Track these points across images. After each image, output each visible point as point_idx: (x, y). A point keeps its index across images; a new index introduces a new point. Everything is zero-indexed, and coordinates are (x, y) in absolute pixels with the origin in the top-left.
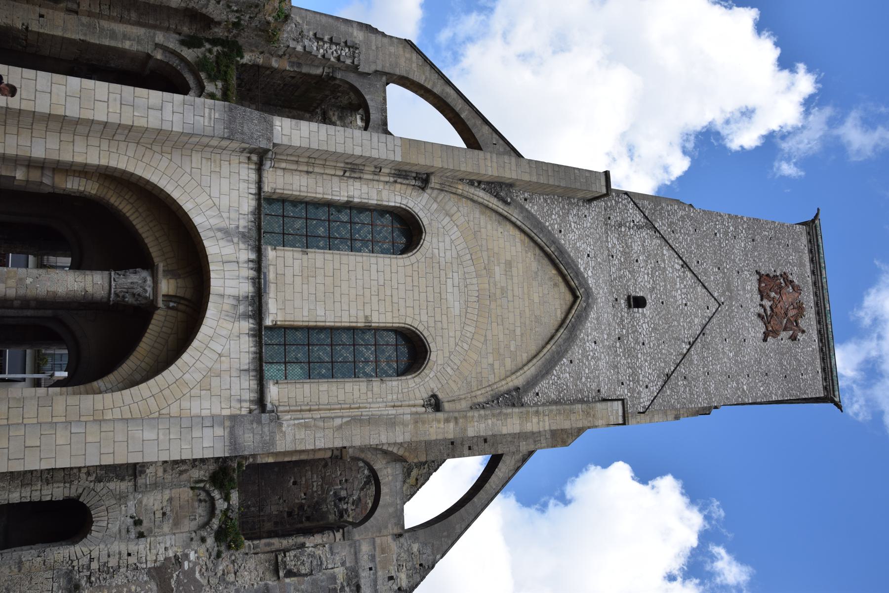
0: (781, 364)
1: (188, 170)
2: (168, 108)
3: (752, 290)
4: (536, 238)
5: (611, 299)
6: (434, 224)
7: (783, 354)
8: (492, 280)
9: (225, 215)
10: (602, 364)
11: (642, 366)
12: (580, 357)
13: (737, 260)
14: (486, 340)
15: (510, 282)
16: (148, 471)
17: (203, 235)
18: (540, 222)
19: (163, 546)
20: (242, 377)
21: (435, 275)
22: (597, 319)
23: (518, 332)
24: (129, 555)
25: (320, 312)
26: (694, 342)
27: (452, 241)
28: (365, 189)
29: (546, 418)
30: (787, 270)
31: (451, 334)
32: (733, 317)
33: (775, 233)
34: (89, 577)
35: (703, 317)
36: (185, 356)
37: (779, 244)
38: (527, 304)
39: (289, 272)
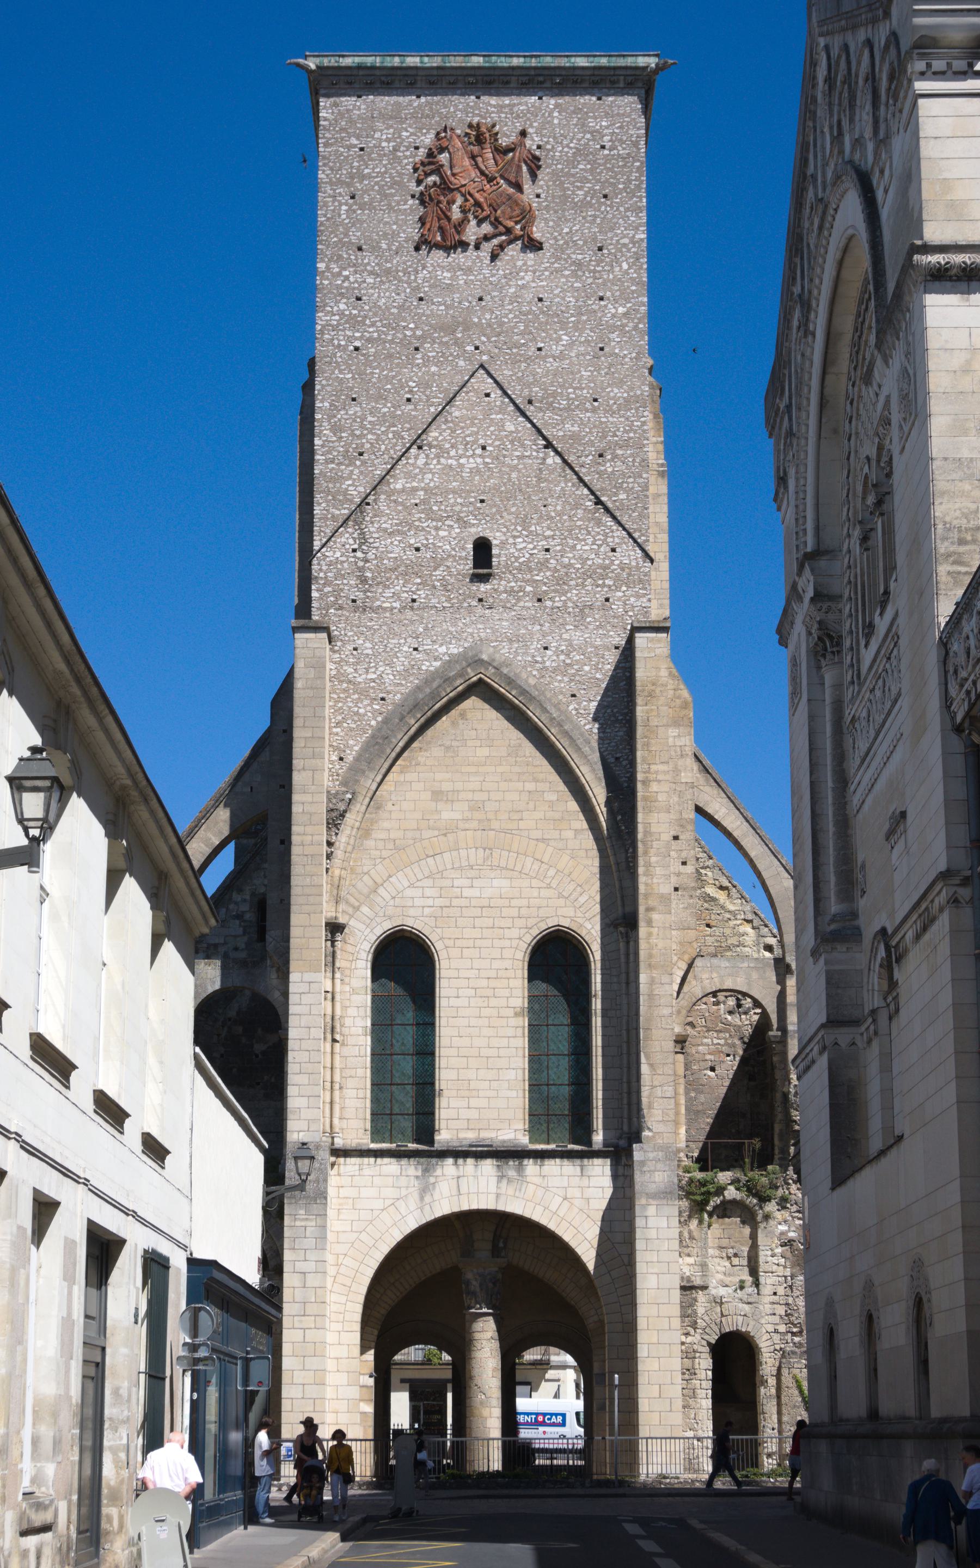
0: (585, 205)
1: (355, 1235)
2: (301, 1266)
3: (451, 269)
4: (398, 749)
5: (479, 610)
6: (390, 911)
7: (564, 198)
8: (461, 825)
9: (404, 1192)
10: (577, 637)
11: (581, 557)
12: (566, 679)
13: (399, 299)
14: (543, 840)
15: (462, 796)
16: (688, 1274)
17: (429, 1217)
18: (373, 736)
19: (770, 1259)
20: (589, 1173)
21: (459, 914)
22: (511, 641)
23: (530, 786)
24: (775, 1294)
25: (511, 1075)
26: (545, 438)
27: (412, 886)
28: (352, 1012)
29: (653, 768)
30: (409, 159)
31: (535, 893)
32: (501, 324)
33: (340, 182)
34: (793, 1334)
35: (502, 411)
36: (567, 1237)
37: (363, 177)
38: (492, 769)
39: (465, 1114)
